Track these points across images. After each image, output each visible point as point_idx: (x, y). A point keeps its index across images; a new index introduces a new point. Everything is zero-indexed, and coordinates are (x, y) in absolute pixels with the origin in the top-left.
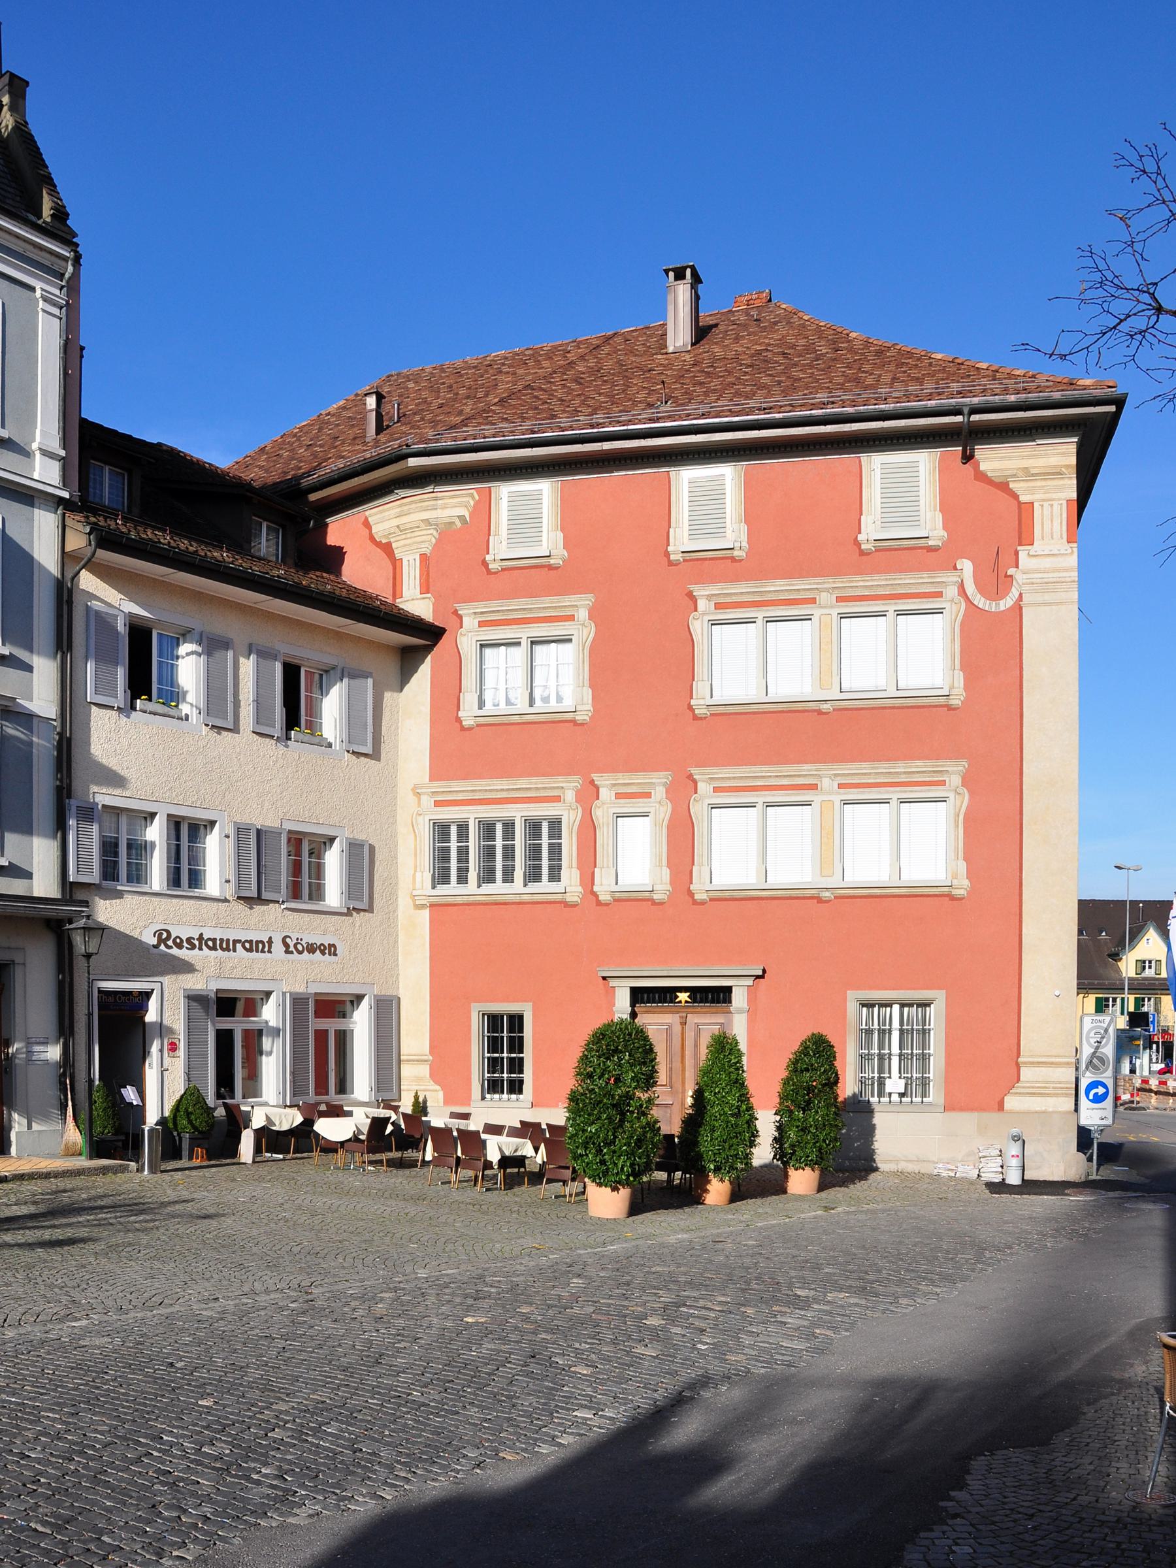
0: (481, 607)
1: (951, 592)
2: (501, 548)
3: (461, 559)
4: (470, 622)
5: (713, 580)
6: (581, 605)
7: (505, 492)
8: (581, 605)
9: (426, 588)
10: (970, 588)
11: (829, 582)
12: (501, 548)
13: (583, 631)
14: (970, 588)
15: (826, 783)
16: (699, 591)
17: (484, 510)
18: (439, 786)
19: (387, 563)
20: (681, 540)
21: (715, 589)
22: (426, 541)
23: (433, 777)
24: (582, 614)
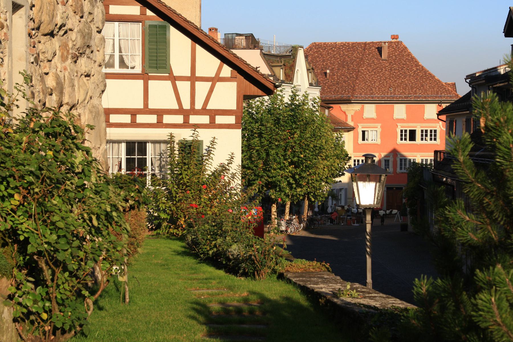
0: (362, 124)
1: (438, 127)
2: (366, 115)
3: (359, 116)
4: (360, 127)
5: (400, 123)
6: (379, 125)
7: (366, 106)
8: (379, 125)
9: (352, 120)
10: (441, 126)
11: (419, 124)
12: (366, 115)
13: (379, 130)
14: (441, 126)
15: (418, 156)
16: (398, 124)
17: (363, 108)
18: (355, 154)
19: (345, 116)
20: (396, 116)
21: (401, 124)
22: (353, 113)
23: (354, 152)
24: (379, 127)
